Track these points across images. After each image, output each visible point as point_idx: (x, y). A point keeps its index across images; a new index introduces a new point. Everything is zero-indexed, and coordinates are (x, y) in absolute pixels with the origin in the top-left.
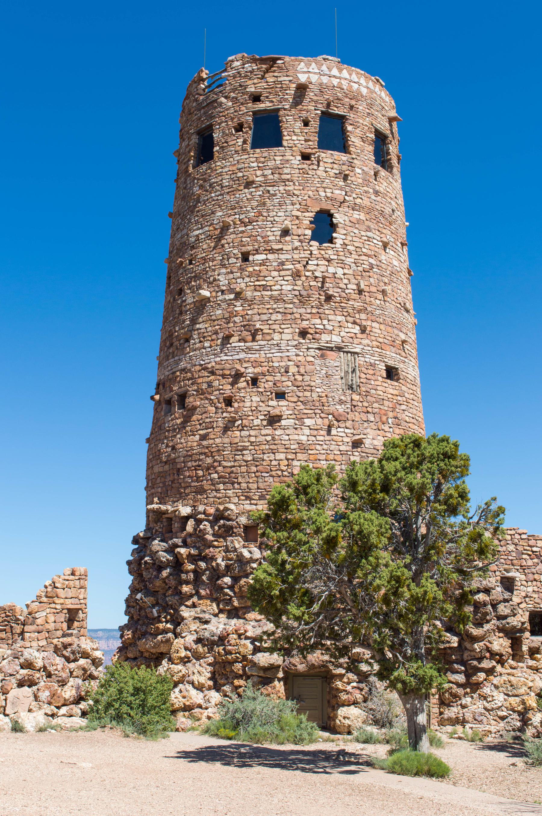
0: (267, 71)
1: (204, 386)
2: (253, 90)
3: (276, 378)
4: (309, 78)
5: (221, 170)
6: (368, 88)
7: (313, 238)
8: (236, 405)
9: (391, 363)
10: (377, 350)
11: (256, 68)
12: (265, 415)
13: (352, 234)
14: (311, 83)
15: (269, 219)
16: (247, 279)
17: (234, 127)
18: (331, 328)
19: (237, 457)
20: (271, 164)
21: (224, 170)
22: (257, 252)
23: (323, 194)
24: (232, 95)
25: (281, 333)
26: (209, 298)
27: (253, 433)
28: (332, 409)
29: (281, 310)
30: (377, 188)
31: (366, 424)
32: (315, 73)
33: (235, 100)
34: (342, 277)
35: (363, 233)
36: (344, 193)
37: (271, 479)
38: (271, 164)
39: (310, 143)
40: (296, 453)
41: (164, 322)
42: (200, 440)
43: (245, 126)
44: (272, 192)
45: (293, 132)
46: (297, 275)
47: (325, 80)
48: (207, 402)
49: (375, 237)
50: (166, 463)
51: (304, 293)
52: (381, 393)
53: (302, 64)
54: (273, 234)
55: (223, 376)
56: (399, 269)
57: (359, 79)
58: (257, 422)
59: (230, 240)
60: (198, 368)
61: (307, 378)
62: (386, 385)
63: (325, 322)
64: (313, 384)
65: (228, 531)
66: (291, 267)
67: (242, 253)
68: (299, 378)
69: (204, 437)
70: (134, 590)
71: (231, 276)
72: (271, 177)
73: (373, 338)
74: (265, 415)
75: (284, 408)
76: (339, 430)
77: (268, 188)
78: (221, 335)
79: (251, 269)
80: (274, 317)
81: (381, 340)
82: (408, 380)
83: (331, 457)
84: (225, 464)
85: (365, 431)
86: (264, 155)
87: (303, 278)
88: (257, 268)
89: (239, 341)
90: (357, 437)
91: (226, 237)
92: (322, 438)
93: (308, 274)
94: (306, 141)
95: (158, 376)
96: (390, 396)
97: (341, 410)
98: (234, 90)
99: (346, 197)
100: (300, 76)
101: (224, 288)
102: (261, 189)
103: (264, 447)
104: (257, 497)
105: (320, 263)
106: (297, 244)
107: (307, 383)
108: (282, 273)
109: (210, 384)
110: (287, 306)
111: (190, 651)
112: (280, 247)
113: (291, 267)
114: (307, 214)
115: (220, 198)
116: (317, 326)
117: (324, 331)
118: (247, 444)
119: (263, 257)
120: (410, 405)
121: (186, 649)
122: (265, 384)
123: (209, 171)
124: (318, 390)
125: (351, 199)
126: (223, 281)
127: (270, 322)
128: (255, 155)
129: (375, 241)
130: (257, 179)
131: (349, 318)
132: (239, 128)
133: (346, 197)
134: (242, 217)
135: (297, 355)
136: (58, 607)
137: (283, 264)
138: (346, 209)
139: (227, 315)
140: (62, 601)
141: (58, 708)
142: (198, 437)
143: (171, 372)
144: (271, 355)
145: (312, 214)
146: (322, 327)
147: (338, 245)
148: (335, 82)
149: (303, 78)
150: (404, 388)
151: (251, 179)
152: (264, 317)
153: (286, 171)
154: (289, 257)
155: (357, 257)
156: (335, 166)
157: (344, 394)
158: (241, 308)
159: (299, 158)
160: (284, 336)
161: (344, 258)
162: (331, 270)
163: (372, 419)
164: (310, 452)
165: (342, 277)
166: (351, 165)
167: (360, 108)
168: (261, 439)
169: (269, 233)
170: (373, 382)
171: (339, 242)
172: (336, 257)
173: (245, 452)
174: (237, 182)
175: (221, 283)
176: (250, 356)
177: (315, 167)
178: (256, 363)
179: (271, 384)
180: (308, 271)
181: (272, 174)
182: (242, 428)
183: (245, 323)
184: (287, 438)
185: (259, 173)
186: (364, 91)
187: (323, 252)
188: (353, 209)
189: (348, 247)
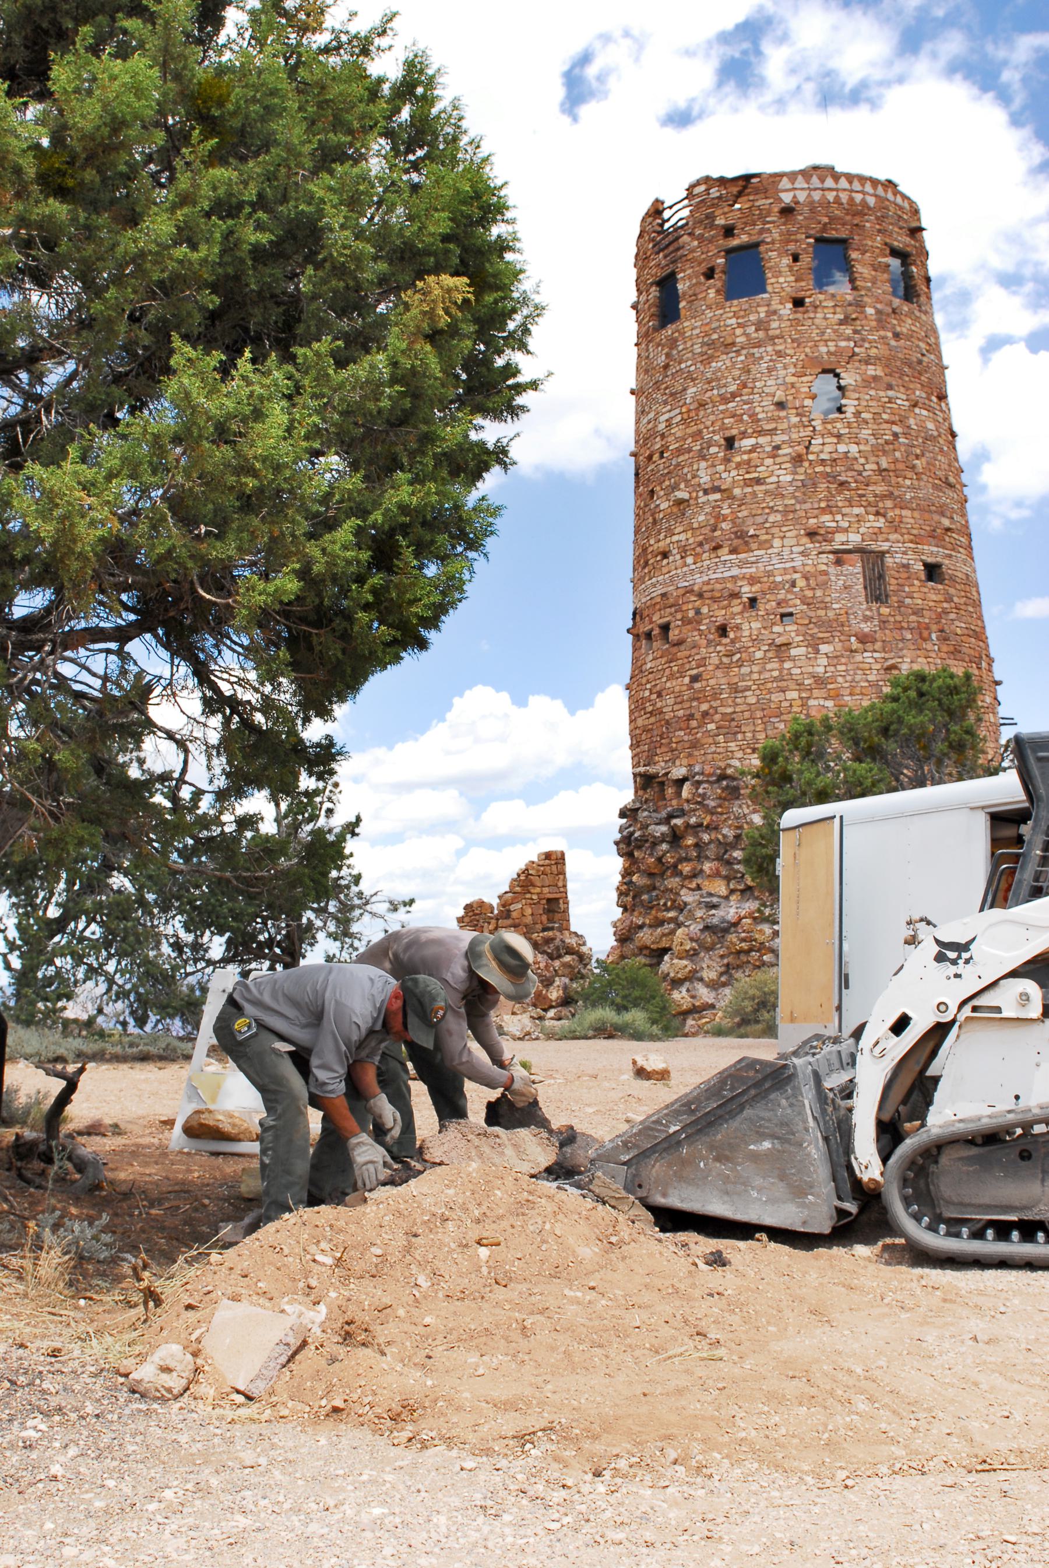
0: (740, 194)
1: (691, 614)
3: (780, 597)
4: (795, 197)
6: (876, 196)
8: (732, 635)
9: (930, 560)
14: (797, 203)
16: (734, 473)
18: (846, 525)
19: (738, 700)
20: (753, 318)
21: (695, 332)
22: (744, 435)
27: (755, 668)
28: (855, 628)
30: (898, 329)
33: (700, 238)
35: (882, 394)
36: (852, 344)
38: (753, 318)
39: (803, 284)
40: (811, 690)
41: (636, 533)
47: (817, 196)
48: (696, 633)
49: (899, 395)
50: (651, 713)
51: (809, 482)
52: (919, 602)
53: (785, 179)
54: (764, 409)
55: (714, 599)
56: (935, 433)
57: (863, 185)
58: (759, 655)
60: (681, 592)
61: (819, 593)
64: (828, 599)
65: (734, 793)
68: (809, 594)
70: (627, 873)
76: (866, 654)
77: (752, 351)
78: (707, 547)
79: (738, 459)
80: (771, 519)
81: (915, 532)
83: (858, 690)
84: (722, 710)
87: (806, 464)
88: (745, 457)
89: (731, 552)
92: (843, 668)
94: (796, 281)
97: (867, 630)
99: (857, 350)
100: (783, 195)
102: (744, 352)
103: (769, 685)
105: (827, 440)
106: (795, 420)
108: (778, 460)
109: (698, 612)
111: (696, 941)
115: (693, 368)
117: (839, 530)
118: (750, 683)
119: (752, 441)
121: (692, 940)
124: (835, 606)
125: (863, 350)
126: (705, 479)
127: (767, 525)
129: (899, 402)
131: (870, 509)
132: (710, 274)
133: (857, 350)
134: (723, 391)
136: (535, 897)
137: (777, 448)
138: (857, 364)
139: (712, 521)
140: (538, 890)
141: (545, 1010)
142: (687, 680)
144: (771, 568)
146: (834, 524)
147: (849, 415)
148: (831, 196)
149: (787, 198)
150: (952, 591)
152: (759, 520)
154: (785, 438)
156: (838, 309)
157: (870, 609)
159: (790, 305)
160: (786, 542)
162: (842, 448)
163: (909, 636)
164: (830, 686)
166: (859, 305)
167: (868, 225)
168: (767, 675)
170: (907, 589)
171: (850, 410)
173: (748, 693)
176: (744, 571)
177: (812, 315)
178: (753, 580)
181: (757, 330)
184: (798, 671)
185: (738, 331)
186: (871, 201)
187: (829, 426)
188: (867, 363)
189: (863, 415)
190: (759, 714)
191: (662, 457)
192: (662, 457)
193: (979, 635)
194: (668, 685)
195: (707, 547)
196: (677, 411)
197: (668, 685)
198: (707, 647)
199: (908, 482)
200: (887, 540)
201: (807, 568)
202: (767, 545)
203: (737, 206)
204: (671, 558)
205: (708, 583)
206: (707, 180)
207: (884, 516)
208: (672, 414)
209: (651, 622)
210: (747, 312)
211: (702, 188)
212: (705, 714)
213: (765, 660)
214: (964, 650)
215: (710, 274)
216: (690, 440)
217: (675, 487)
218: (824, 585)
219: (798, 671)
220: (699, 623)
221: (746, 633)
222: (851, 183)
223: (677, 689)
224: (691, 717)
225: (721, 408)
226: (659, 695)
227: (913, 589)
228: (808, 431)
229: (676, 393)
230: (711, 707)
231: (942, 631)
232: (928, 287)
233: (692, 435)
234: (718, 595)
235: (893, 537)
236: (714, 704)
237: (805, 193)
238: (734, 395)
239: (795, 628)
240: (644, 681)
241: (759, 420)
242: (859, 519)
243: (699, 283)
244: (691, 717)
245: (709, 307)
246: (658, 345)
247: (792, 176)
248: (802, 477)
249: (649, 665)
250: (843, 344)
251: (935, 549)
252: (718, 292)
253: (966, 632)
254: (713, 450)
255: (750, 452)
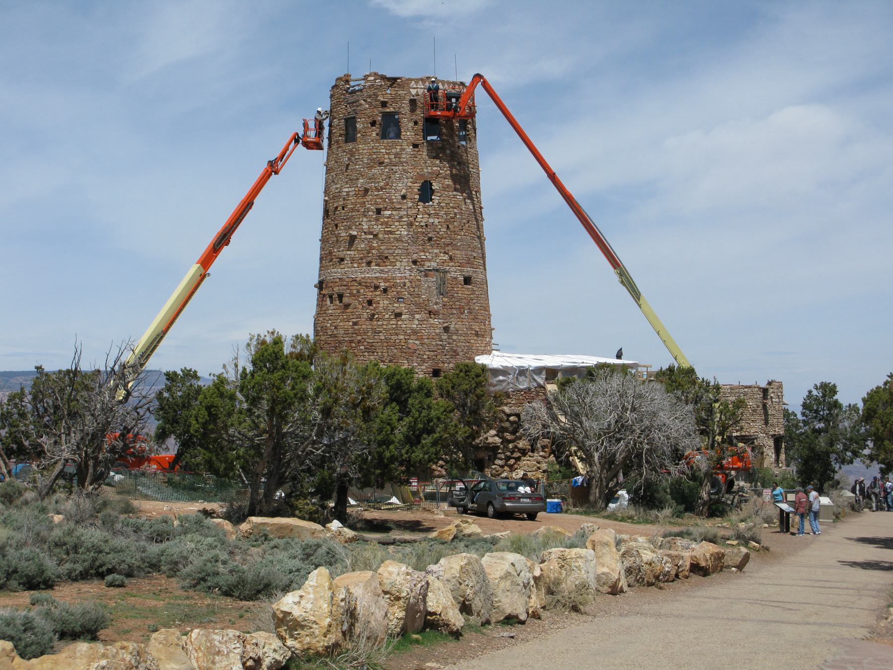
1: (355, 292)
2: (382, 99)
3: (398, 290)
4: (417, 92)
5: (362, 151)
7: (420, 200)
8: (374, 305)
10: (459, 268)
11: (383, 83)
12: (392, 312)
13: (444, 195)
15: (393, 187)
16: (380, 227)
17: (370, 123)
18: (431, 257)
20: (393, 151)
21: (364, 152)
22: (386, 209)
23: (425, 170)
24: (369, 100)
25: (401, 262)
26: (356, 236)
27: (385, 323)
29: (401, 247)
31: (451, 316)
32: (421, 88)
33: (370, 104)
34: (438, 224)
35: (451, 193)
37: (396, 351)
38: (393, 151)
42: (353, 325)
43: (377, 123)
44: (394, 170)
45: (408, 129)
46: (410, 225)
48: (356, 301)
50: (330, 335)
51: (414, 236)
52: (460, 295)
53: (413, 82)
58: (387, 316)
59: (369, 200)
61: (416, 290)
62: (464, 289)
63: (427, 254)
66: (406, 219)
67: (376, 209)
68: (412, 290)
69: (355, 324)
71: (370, 223)
72: (394, 160)
73: (456, 261)
74: (392, 312)
75: (403, 308)
76: (435, 320)
78: (364, 261)
79: (382, 220)
80: (397, 252)
81: (461, 261)
82: (478, 283)
83: (431, 337)
84: (368, 340)
85: (451, 320)
86: (389, 145)
87: (414, 227)
88: (386, 220)
89: (376, 265)
90: (446, 325)
91: (366, 197)
92: (425, 326)
93: (417, 224)
94: (415, 135)
95: (320, 275)
96: (466, 296)
98: (370, 97)
99: (441, 171)
101: (366, 231)
102: (388, 167)
104: (387, 361)
105: (425, 216)
107: (416, 293)
108: (401, 223)
109: (358, 292)
110: (404, 244)
112: (400, 206)
113: (406, 219)
114: (415, 185)
115: (362, 170)
116: (422, 257)
119: (390, 212)
120: (479, 298)
122: (392, 294)
123: (354, 150)
125: (443, 171)
127: (394, 255)
128: (384, 145)
129: (458, 197)
130: (385, 161)
132: (373, 124)
133: (441, 171)
134: (377, 185)
135: (410, 275)
137: (401, 217)
139: (368, 248)
142: (351, 323)
143: (332, 278)
145: (419, 185)
146: (425, 257)
147: (435, 204)
149: (413, 92)
151: (382, 161)
152: (391, 251)
153: (403, 156)
155: (447, 210)
158: (376, 245)
159: (411, 147)
160: (403, 264)
161: (438, 212)
162: (431, 220)
163: (455, 312)
165: (438, 224)
168: (390, 326)
169: (393, 197)
170: (455, 289)
172: (433, 212)
173: (380, 334)
174: (373, 161)
175: (364, 227)
176: (382, 275)
178: (386, 280)
179: (395, 293)
180: (417, 222)
181: (395, 158)
182: (378, 320)
183: (379, 254)
184: (405, 326)
185: (386, 156)
187: (426, 209)
189: (441, 204)
190: (385, 344)
191: (343, 209)
192: (343, 209)
193: (486, 308)
194: (341, 324)
195: (364, 261)
196: (353, 189)
197: (341, 324)
198: (362, 309)
199: (459, 237)
200: (448, 266)
201: (412, 277)
202: (393, 264)
203: (388, 91)
204: (346, 262)
205: (364, 278)
206: (376, 74)
207: (448, 254)
208: (350, 189)
209: (333, 291)
210: (391, 147)
211: (372, 78)
212: (359, 342)
213: (389, 319)
214: (479, 317)
215: (373, 124)
216: (358, 206)
217: (350, 228)
218: (419, 286)
219: (405, 326)
220: (358, 297)
221: (382, 305)
222: (443, 86)
223: (346, 327)
224: (351, 342)
225: (376, 193)
226: (336, 328)
227: (459, 289)
228: (415, 211)
229: (352, 180)
230: (363, 338)
231: (469, 309)
232: (475, 133)
233: (360, 203)
234: (369, 285)
235: (451, 264)
236: (364, 337)
237: (422, 90)
238: (382, 189)
239: (404, 305)
240: (327, 318)
241: (393, 203)
242: (437, 255)
243: (367, 128)
244: (351, 342)
245: (372, 140)
246: (344, 152)
247: (417, 81)
248: (412, 233)
249: (331, 311)
250: (435, 168)
251: (469, 269)
252: (377, 134)
253: (481, 308)
254: (371, 213)
255: (388, 218)
